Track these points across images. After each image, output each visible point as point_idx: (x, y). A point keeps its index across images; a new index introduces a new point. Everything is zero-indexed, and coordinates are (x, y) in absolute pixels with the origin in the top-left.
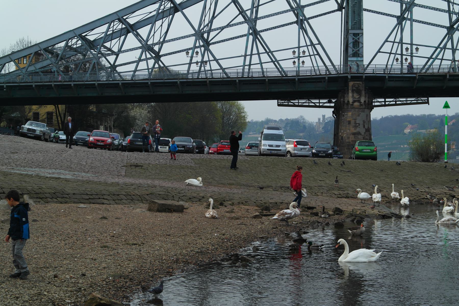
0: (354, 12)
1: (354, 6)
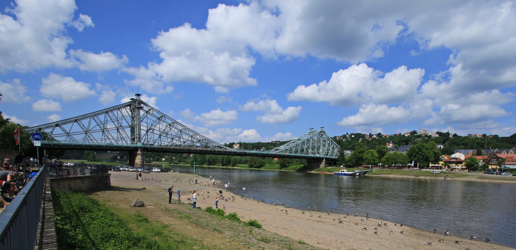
0: (138, 130)
1: (139, 128)
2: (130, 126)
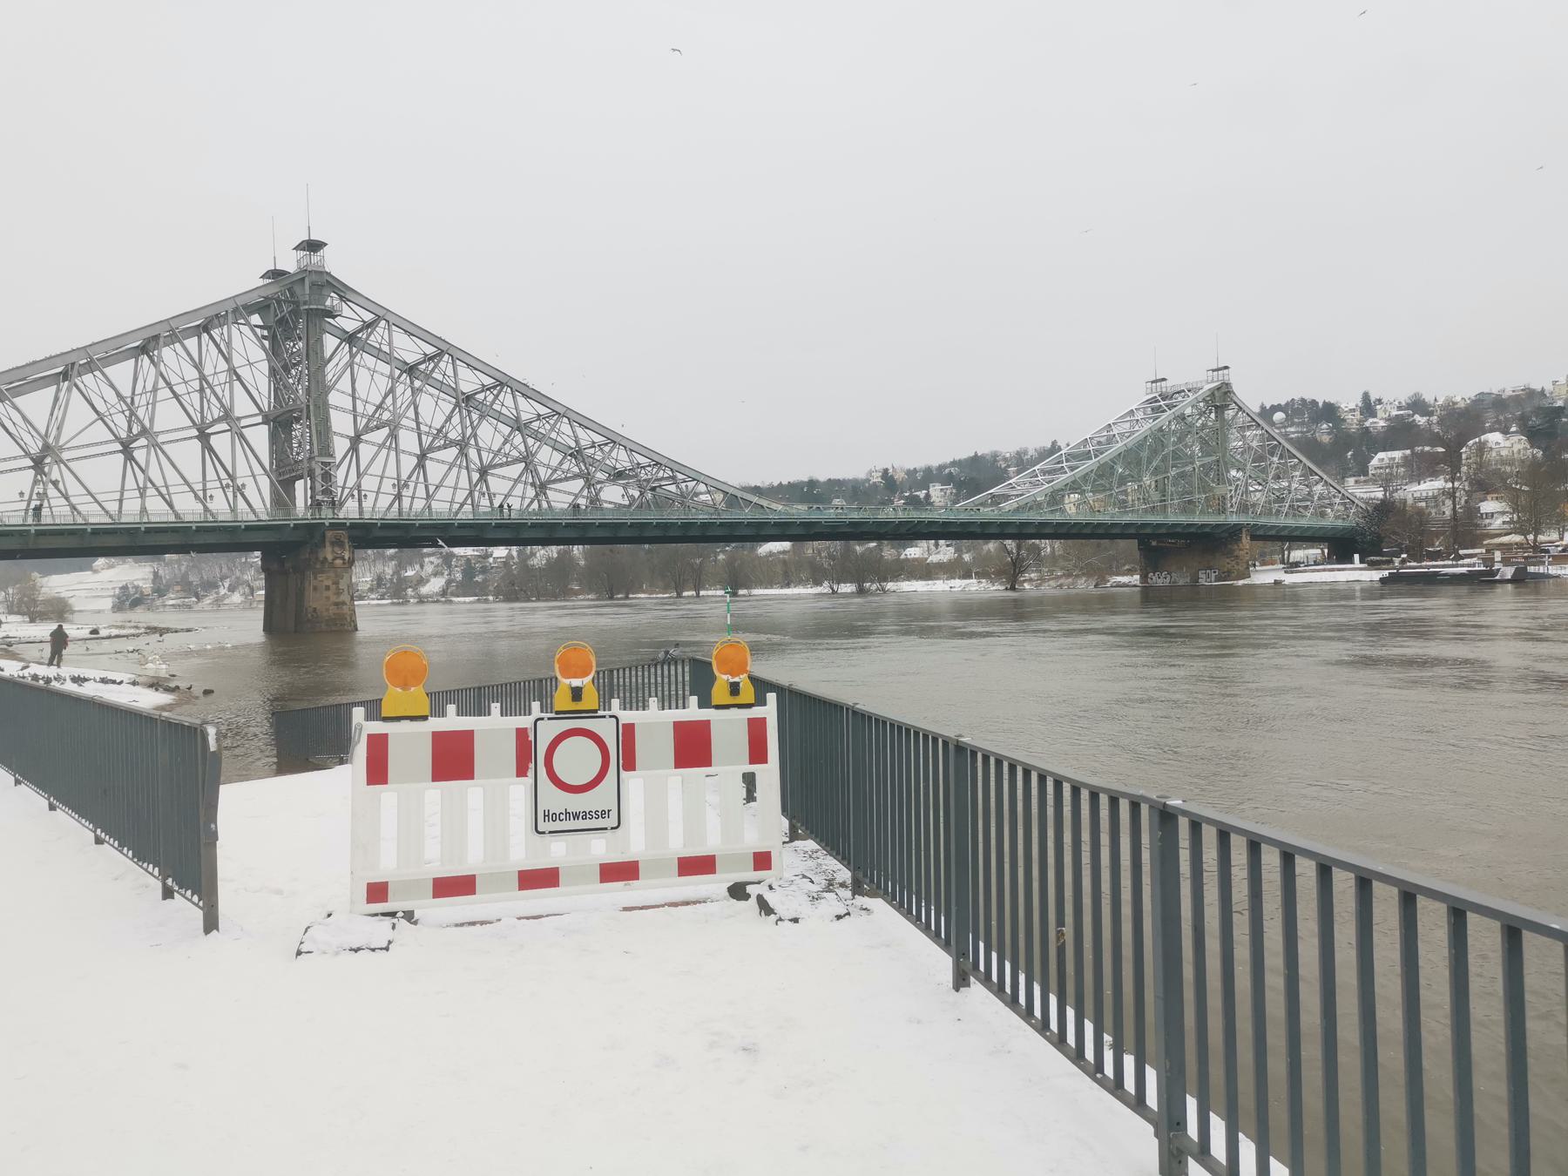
0: (319, 433)
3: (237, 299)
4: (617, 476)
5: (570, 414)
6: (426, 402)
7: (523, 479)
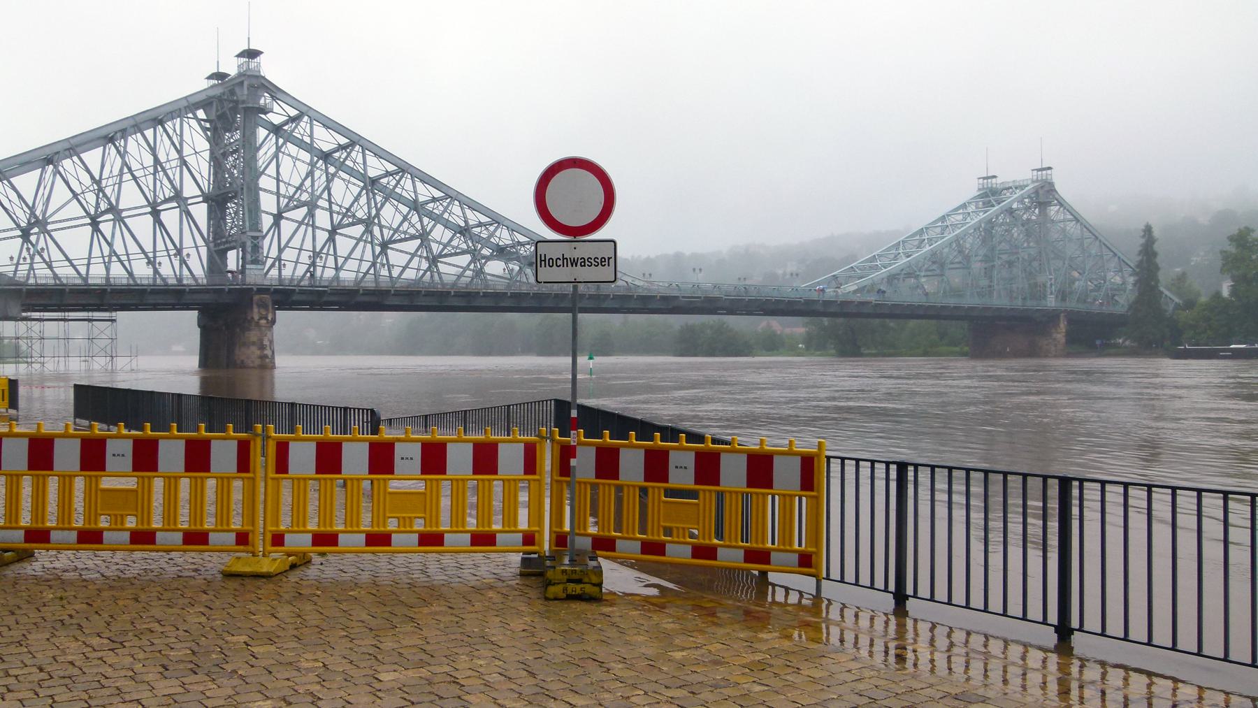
0: (250, 211)
2: (206, 198)
3: (189, 99)
4: (501, 252)
5: (461, 198)
6: (337, 186)
7: (419, 253)
